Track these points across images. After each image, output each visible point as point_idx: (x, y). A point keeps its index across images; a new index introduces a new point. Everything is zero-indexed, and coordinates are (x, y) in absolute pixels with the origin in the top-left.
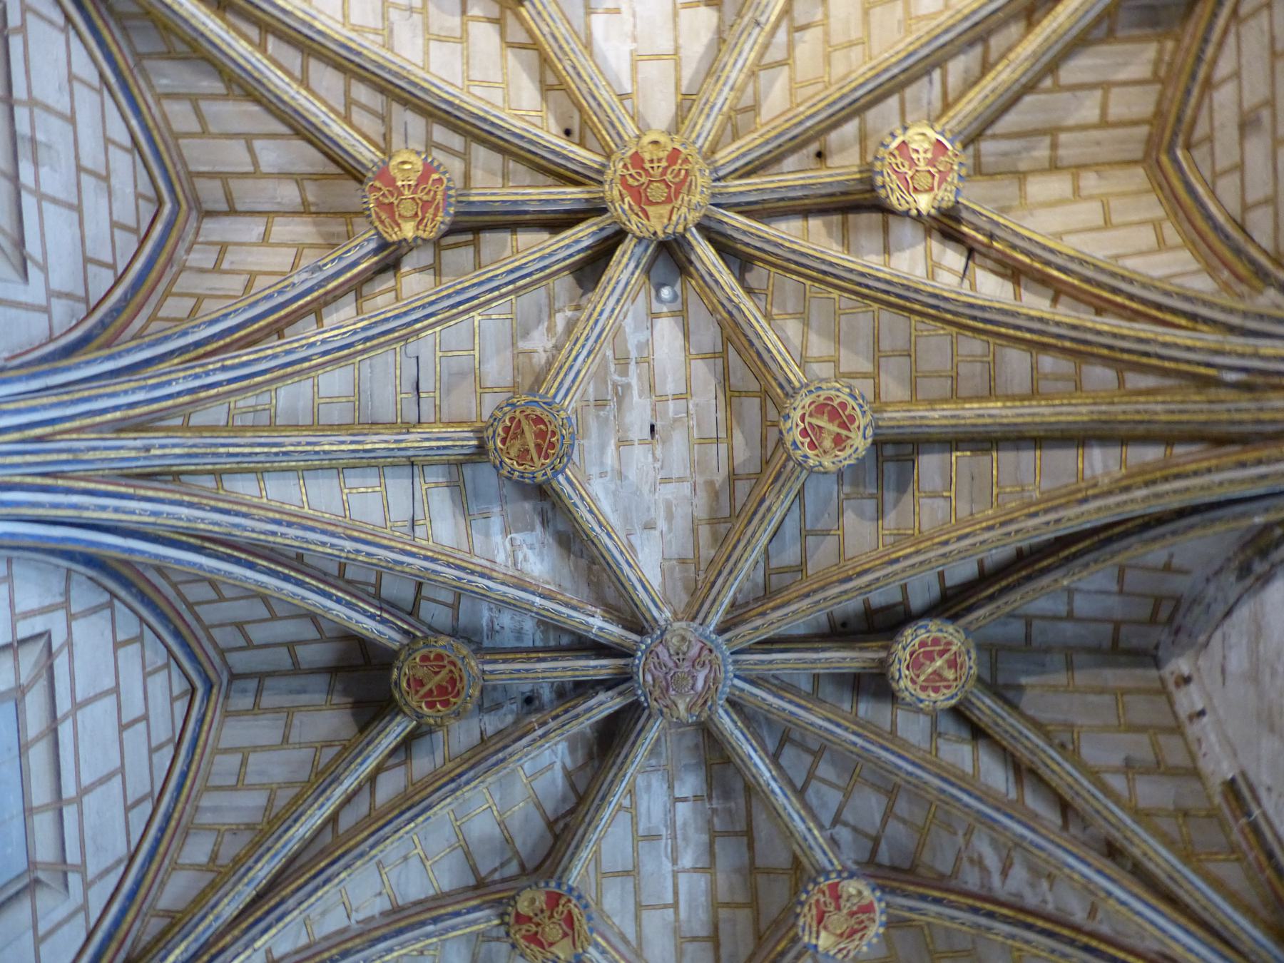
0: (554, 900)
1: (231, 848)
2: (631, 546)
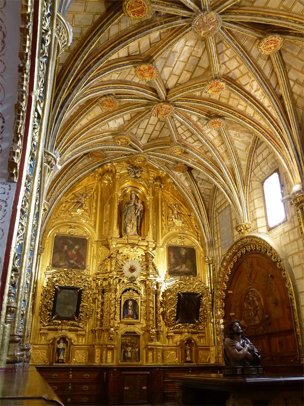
0: (150, 68)
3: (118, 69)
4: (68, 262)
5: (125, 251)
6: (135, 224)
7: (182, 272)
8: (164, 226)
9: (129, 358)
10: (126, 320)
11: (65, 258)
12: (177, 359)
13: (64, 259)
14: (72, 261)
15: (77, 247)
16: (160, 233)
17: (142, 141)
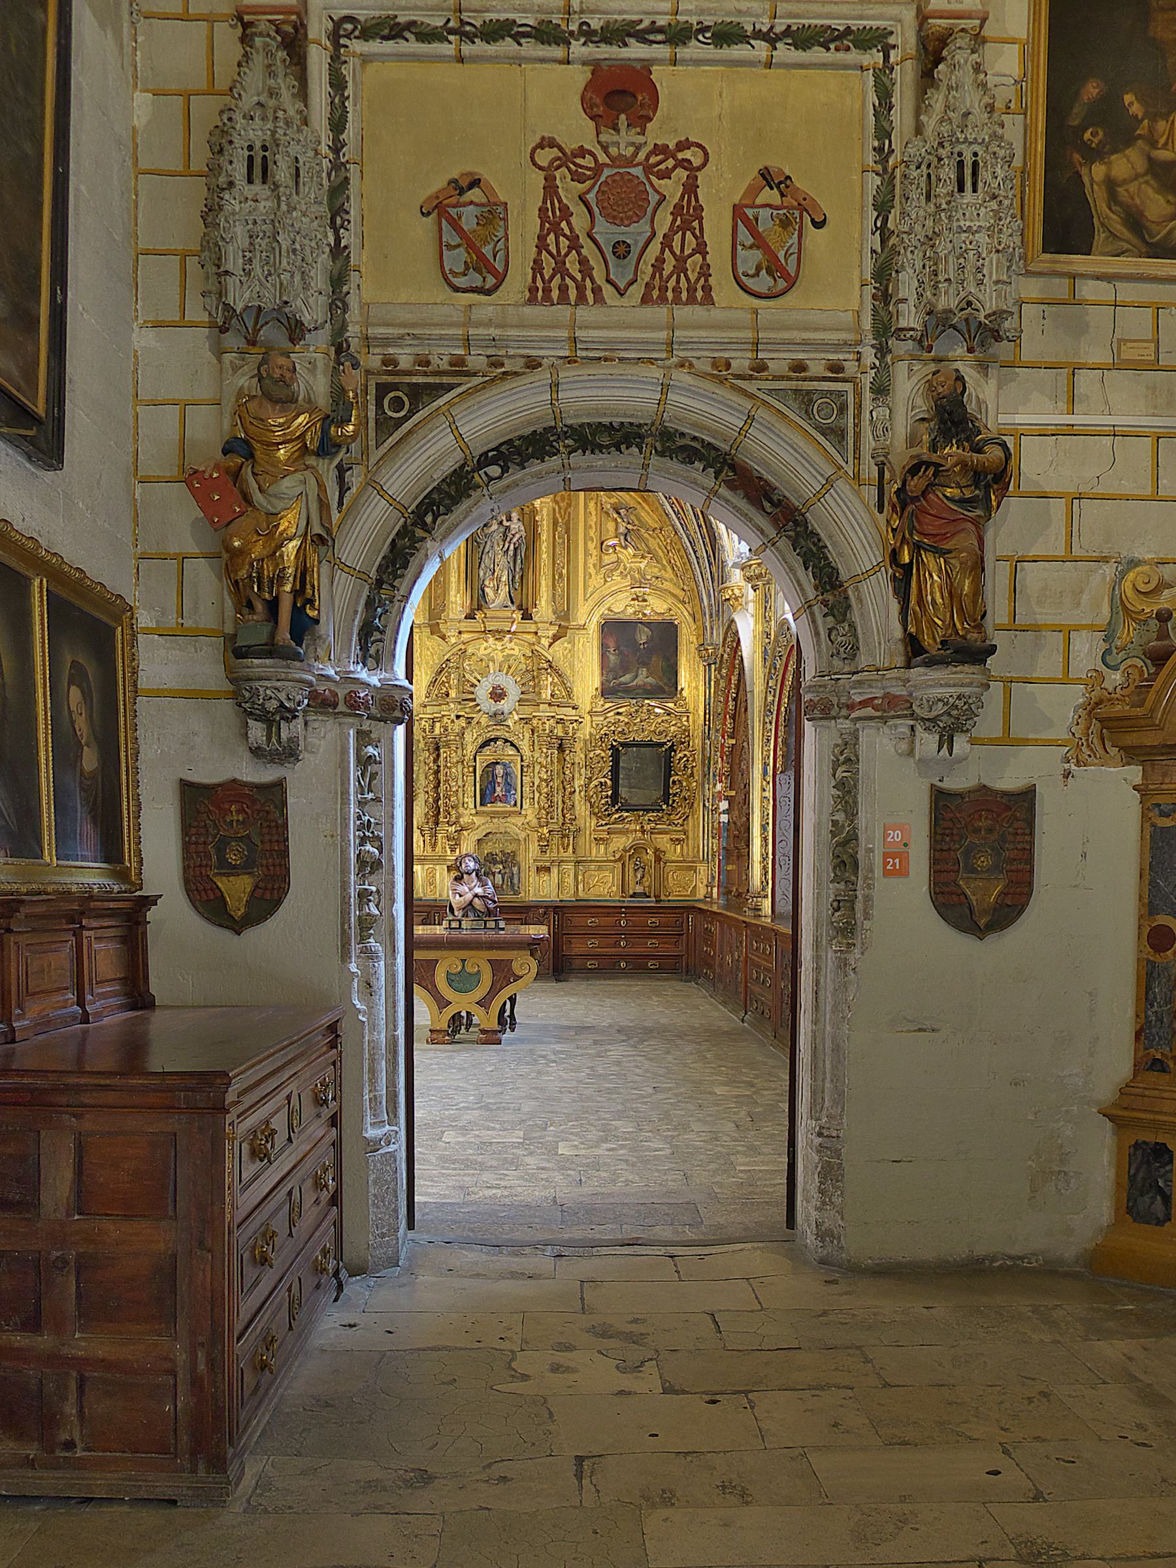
5: (489, 647)
6: (504, 578)
7: (638, 687)
8: (592, 570)
10: (489, 808)
12: (614, 889)
16: (581, 591)
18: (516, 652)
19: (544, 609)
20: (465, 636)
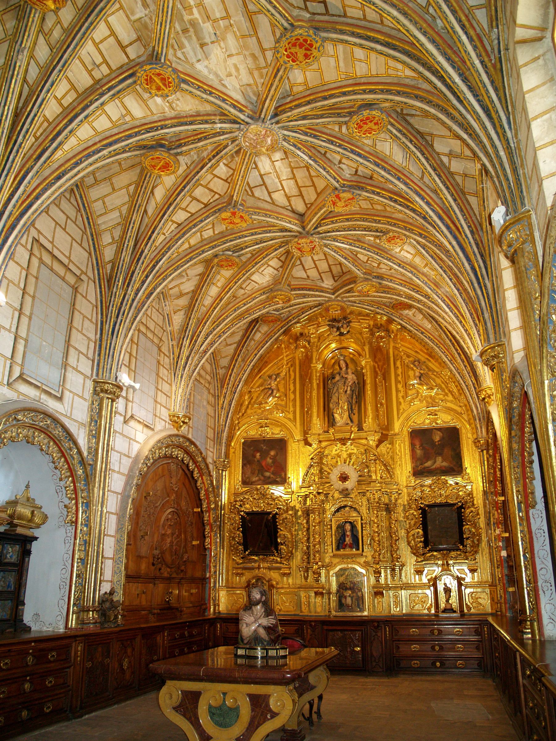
0: (234, 214)
1: (117, 233)
2: (224, 85)
3: (194, 230)
4: (262, 475)
6: (346, 407)
7: (436, 469)
8: (401, 400)
9: (348, 606)
10: (342, 552)
11: (259, 470)
13: (257, 472)
14: (267, 474)
15: (272, 453)
17: (326, 282)
18: (355, 451)
19: (369, 422)
20: (324, 444)
